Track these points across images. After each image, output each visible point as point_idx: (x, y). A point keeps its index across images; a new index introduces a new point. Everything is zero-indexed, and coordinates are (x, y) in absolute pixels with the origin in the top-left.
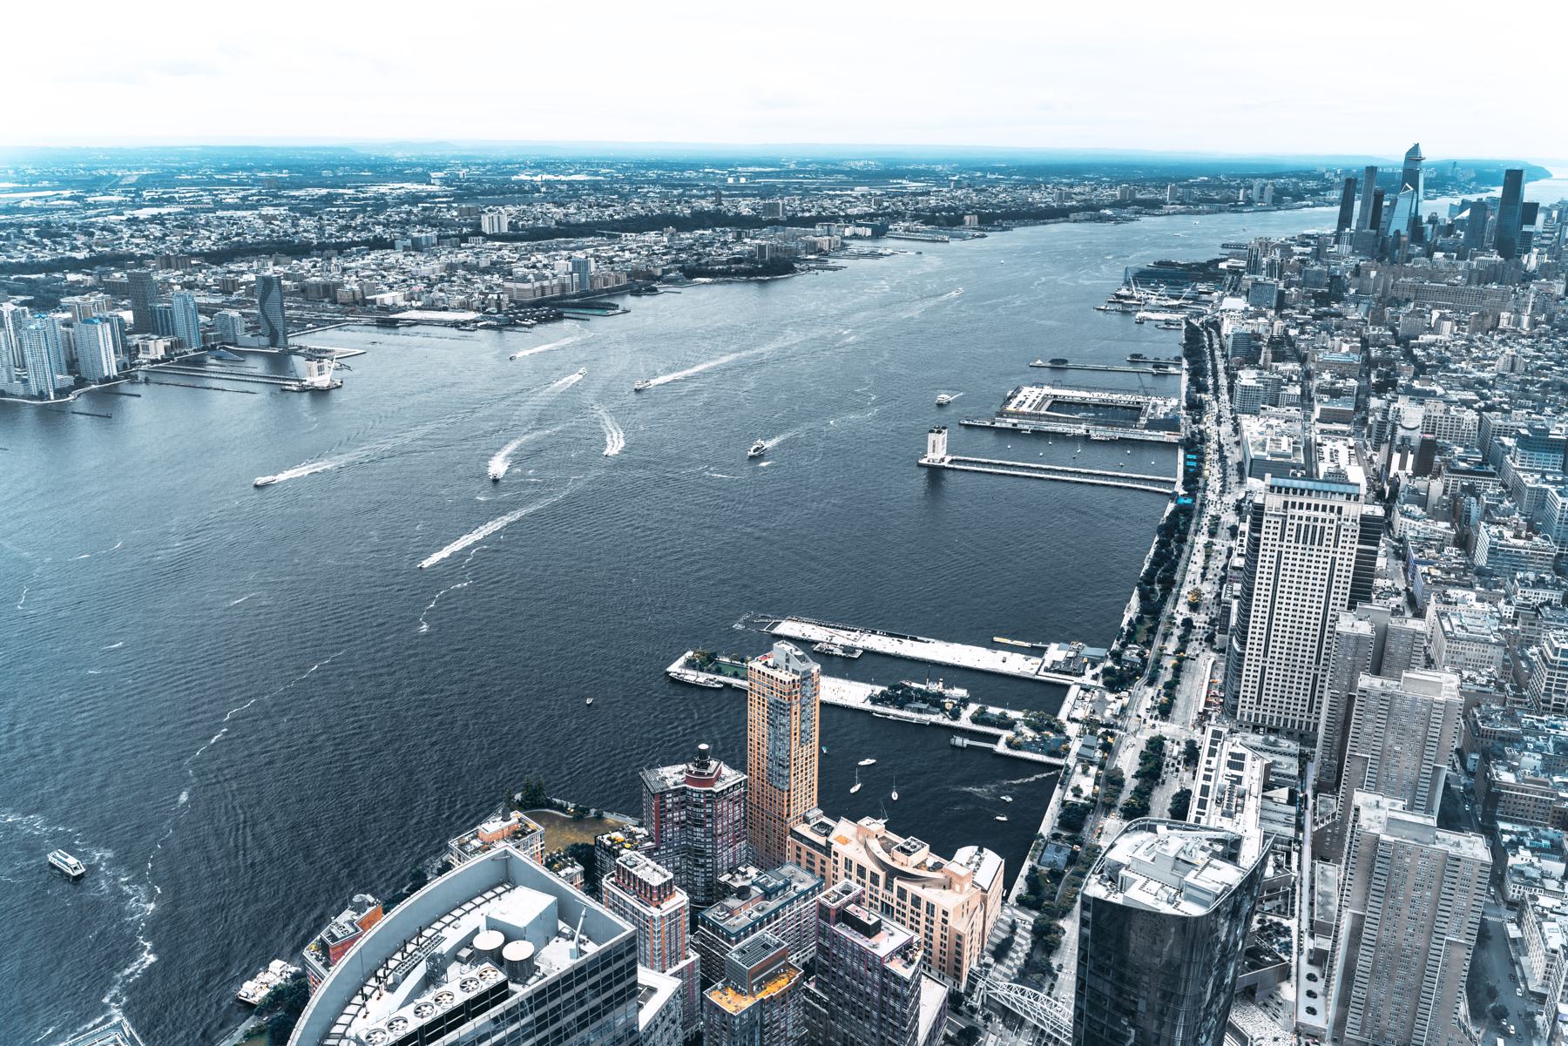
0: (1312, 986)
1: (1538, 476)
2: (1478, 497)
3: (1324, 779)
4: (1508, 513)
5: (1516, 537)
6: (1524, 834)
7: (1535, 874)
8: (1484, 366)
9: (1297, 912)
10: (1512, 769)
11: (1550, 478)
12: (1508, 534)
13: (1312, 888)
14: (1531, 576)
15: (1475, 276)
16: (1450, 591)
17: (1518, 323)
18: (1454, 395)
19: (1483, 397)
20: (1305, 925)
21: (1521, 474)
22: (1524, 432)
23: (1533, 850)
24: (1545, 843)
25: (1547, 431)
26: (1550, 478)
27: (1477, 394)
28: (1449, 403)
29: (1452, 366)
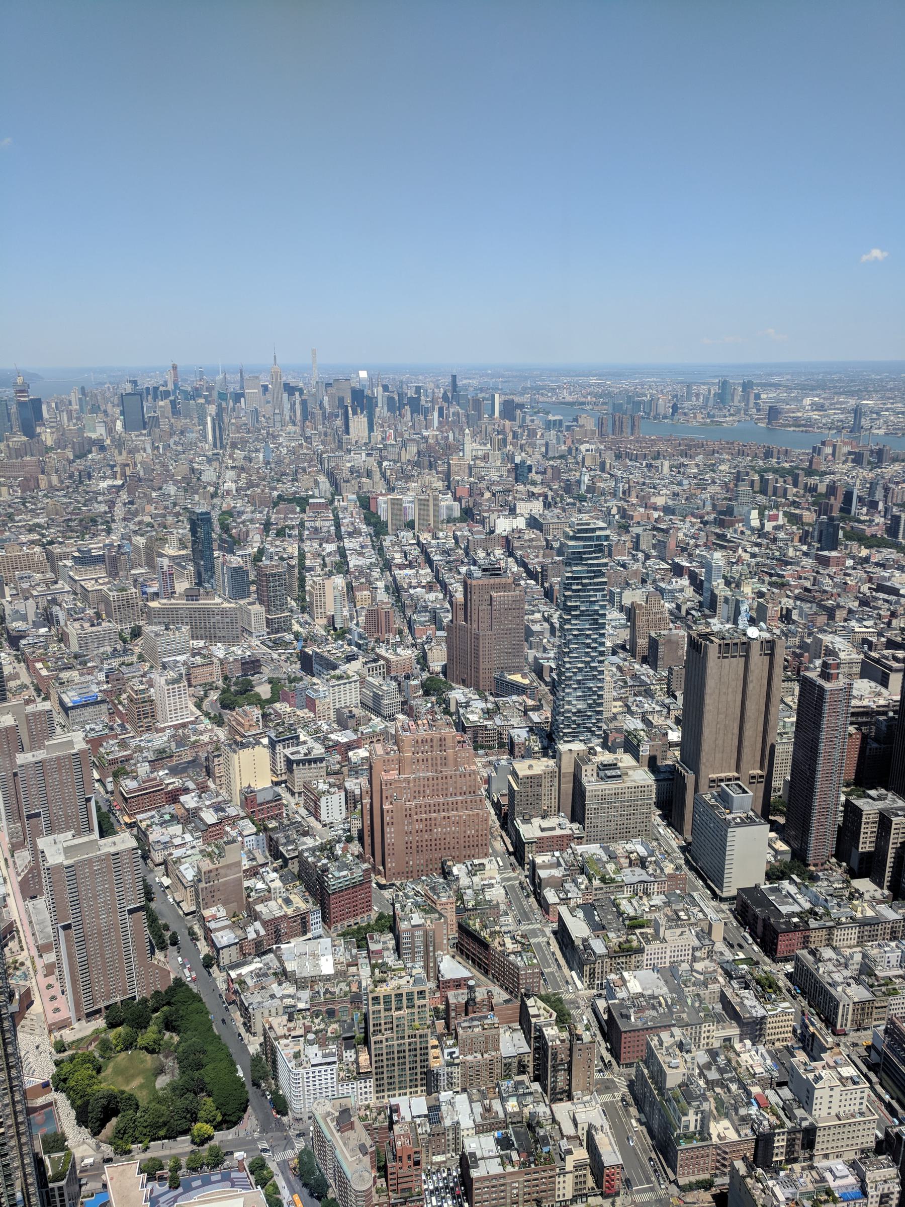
0: (52, 992)
1: (93, 582)
2: (60, 605)
3: (14, 840)
4: (83, 610)
5: (93, 625)
6: (153, 817)
7: (167, 839)
8: (38, 514)
9: (25, 947)
10: (135, 778)
11: (101, 581)
12: (87, 625)
13: (31, 922)
14: (109, 649)
15: (13, 452)
16: (62, 675)
17: (50, 482)
18: (23, 538)
19: (43, 536)
20: (34, 952)
21: (83, 583)
22: (76, 554)
23: (161, 825)
24: (167, 817)
25: (89, 551)
26: (101, 581)
27: (39, 534)
28: (22, 544)
29: (17, 518)
